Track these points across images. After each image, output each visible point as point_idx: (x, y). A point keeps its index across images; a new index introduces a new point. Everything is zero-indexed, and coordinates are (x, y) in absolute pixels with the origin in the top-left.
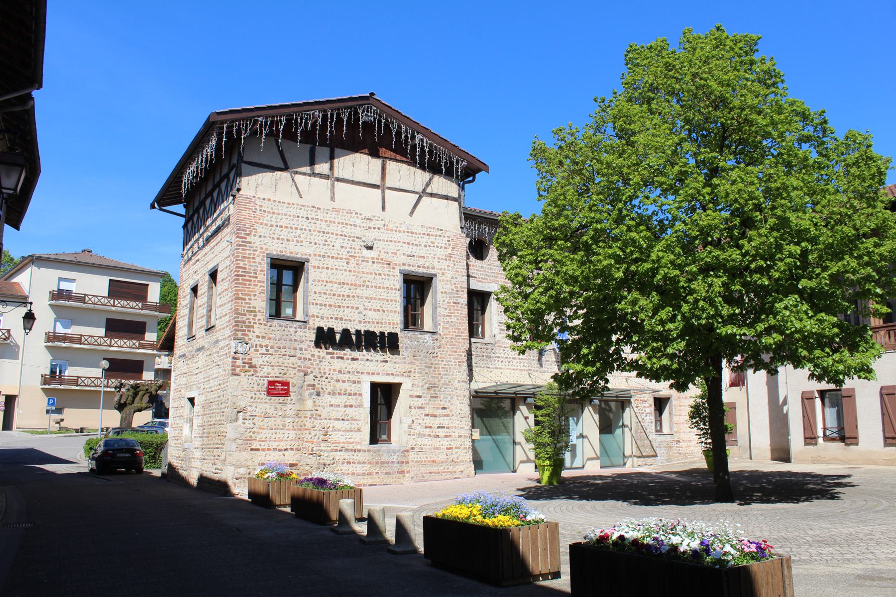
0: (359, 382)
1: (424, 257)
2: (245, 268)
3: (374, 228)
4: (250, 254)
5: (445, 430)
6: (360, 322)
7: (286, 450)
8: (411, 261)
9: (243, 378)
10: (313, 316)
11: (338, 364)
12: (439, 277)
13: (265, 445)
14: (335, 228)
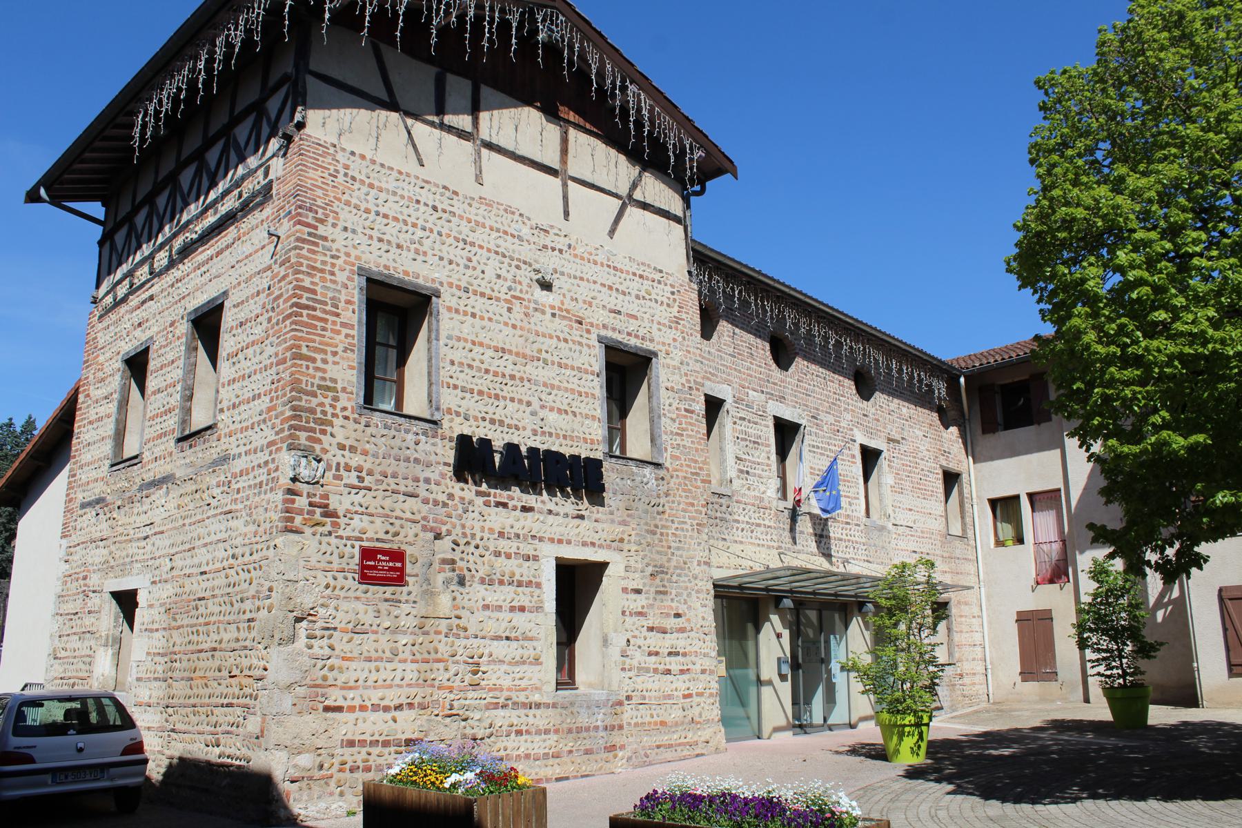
0: (536, 558)
1: (635, 317)
2: (314, 292)
3: (553, 249)
4: (324, 263)
5: (680, 658)
6: (535, 433)
7: (399, 707)
9: (310, 541)
10: (449, 411)
11: (498, 519)
13: (354, 698)
14: (485, 237)
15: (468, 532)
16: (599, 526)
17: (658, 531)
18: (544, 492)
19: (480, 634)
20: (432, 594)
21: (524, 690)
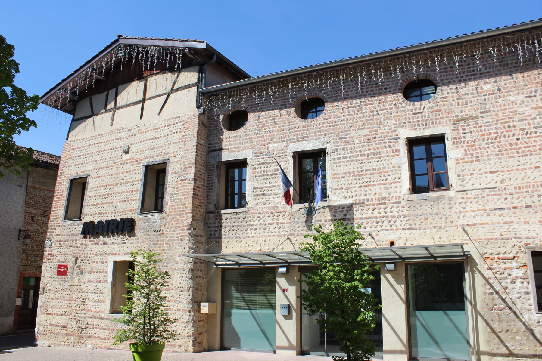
8: (152, 153)
11: (96, 249)
12: (171, 161)
15: (86, 255)
16: (132, 245)
20: (73, 278)
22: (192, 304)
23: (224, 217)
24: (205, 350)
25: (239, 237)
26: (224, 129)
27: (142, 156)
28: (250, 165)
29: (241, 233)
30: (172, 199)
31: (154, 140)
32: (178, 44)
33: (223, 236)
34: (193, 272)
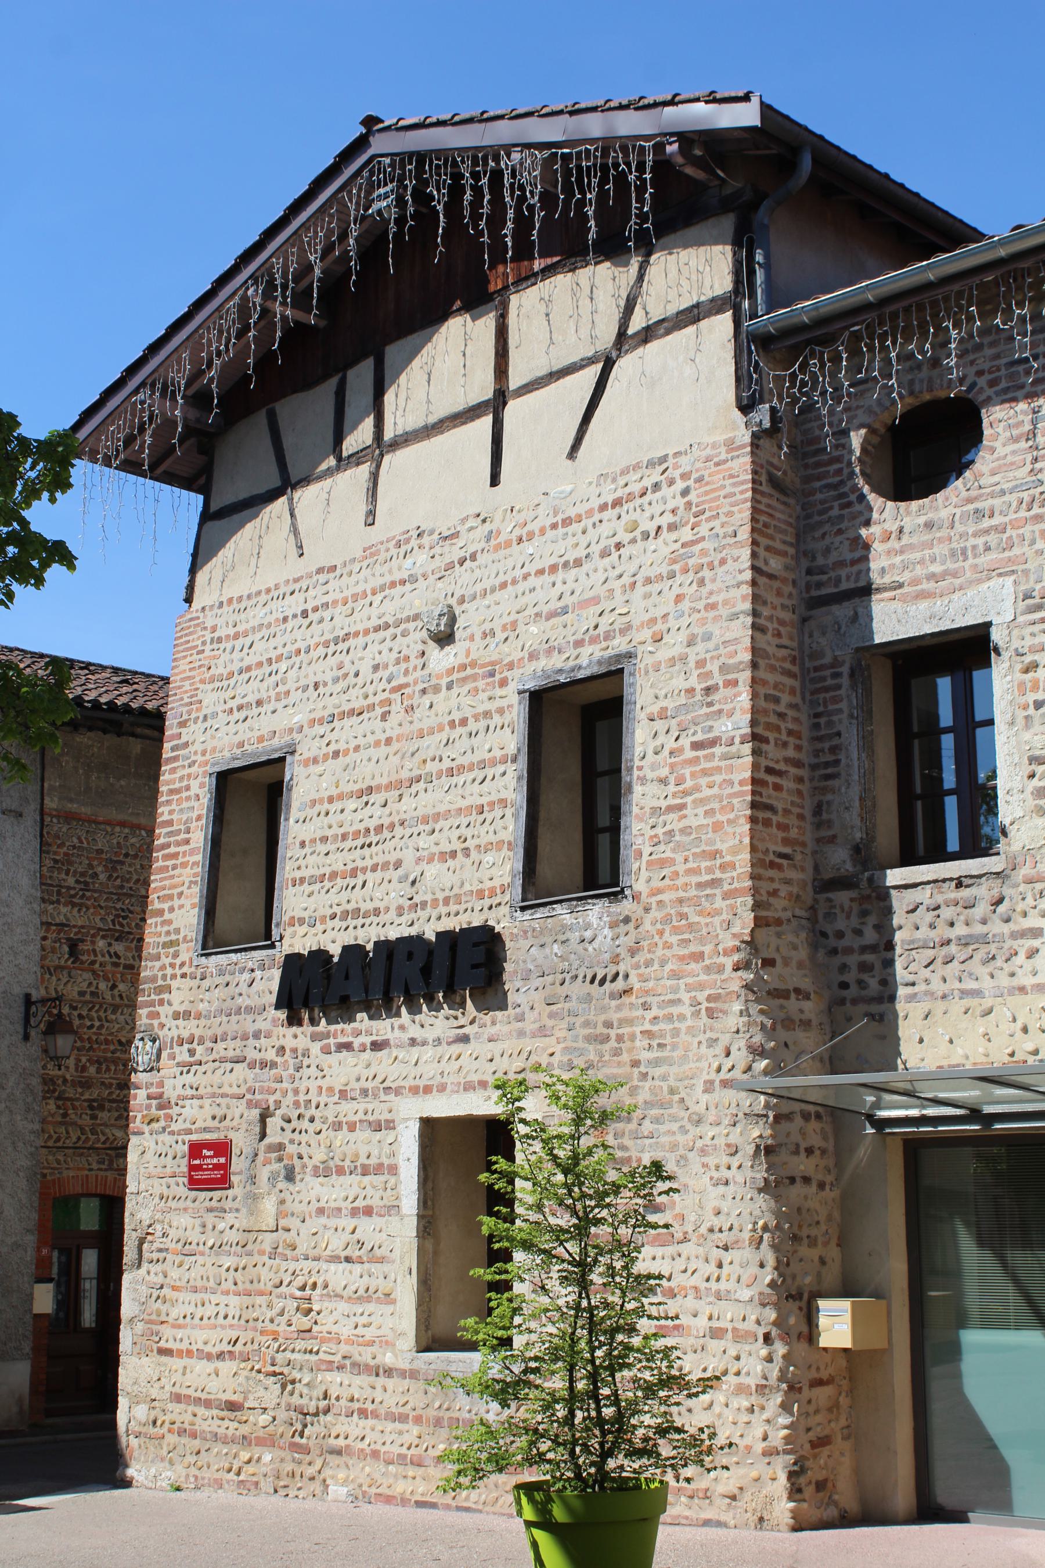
11: (344, 1069)
12: (644, 661)
15: (302, 1098)
16: (496, 1048)
17: (613, 1033)
18: (403, 1010)
19: (312, 1253)
20: (255, 1198)
21: (371, 1343)
22: (777, 1306)
23: (900, 902)
24: (845, 1521)
25: (977, 993)
26: (872, 498)
27: (512, 651)
28: (1005, 655)
29: (983, 971)
30: (660, 831)
31: (561, 574)
32: (629, 124)
33: (902, 992)
34: (773, 1158)
